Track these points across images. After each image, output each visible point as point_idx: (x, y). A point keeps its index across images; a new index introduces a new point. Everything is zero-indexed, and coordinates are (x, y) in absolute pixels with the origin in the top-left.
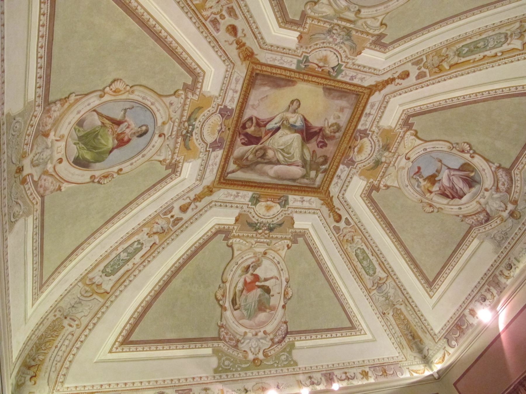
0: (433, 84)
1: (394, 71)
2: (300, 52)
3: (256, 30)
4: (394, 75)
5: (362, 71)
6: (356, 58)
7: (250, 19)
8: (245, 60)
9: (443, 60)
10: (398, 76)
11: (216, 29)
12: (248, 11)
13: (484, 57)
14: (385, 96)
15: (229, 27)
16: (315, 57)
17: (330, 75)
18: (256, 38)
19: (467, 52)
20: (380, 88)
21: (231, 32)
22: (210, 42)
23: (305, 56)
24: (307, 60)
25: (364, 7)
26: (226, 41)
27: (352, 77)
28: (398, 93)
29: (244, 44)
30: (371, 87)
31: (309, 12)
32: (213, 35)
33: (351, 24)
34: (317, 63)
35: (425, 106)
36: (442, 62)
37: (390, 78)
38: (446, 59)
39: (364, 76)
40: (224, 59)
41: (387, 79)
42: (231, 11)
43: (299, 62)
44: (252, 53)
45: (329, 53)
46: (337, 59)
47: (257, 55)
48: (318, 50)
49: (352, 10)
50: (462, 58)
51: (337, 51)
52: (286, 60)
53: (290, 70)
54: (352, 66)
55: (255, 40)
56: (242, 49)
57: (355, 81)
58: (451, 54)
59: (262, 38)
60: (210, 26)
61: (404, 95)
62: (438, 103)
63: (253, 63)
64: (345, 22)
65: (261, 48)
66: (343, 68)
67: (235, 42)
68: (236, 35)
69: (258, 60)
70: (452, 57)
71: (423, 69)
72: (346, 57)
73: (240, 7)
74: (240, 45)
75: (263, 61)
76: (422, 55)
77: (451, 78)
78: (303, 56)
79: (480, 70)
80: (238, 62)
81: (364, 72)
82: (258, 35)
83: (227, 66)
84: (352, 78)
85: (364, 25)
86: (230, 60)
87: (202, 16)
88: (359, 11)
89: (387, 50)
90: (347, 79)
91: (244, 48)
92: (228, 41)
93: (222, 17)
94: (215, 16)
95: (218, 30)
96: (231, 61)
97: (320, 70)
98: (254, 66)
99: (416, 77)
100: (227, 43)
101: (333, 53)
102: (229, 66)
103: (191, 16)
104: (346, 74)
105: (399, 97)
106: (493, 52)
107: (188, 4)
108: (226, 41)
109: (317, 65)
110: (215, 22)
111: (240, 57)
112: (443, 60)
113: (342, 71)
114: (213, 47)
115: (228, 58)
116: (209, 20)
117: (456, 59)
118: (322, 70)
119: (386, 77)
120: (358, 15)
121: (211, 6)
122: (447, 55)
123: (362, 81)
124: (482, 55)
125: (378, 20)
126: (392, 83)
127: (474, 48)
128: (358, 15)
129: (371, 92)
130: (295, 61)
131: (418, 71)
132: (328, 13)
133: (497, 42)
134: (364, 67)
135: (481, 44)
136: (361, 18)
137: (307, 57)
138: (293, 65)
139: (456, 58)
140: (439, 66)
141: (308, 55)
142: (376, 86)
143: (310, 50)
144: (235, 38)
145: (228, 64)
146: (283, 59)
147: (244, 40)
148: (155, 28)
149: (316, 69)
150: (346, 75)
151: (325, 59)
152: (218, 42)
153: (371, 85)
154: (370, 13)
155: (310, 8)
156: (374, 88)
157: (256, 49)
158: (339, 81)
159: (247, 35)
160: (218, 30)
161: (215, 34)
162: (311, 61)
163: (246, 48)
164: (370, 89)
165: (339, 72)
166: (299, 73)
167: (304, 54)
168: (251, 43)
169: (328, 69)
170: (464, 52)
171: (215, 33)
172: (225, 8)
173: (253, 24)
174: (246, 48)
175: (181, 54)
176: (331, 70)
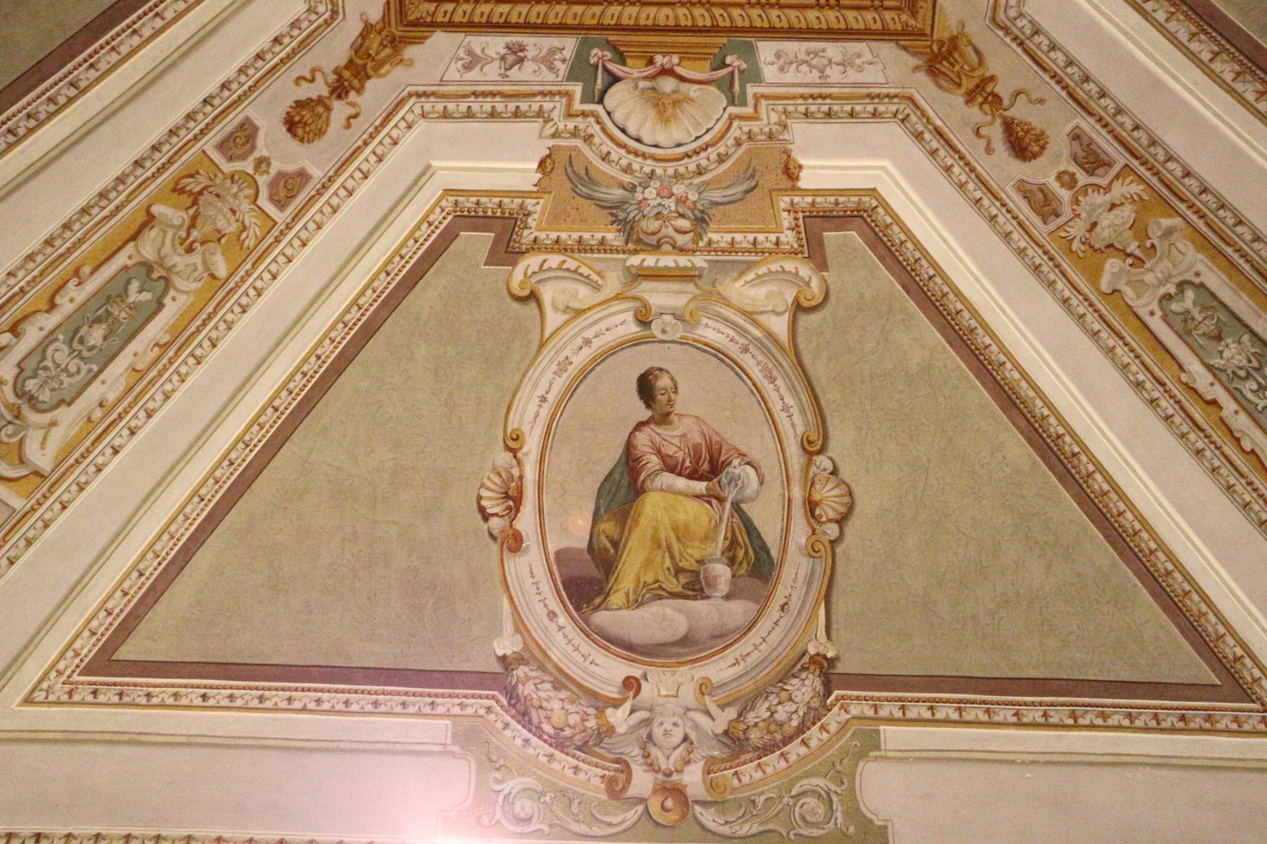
0: (172, 132)
1: (361, 127)
2: (769, 117)
3: (949, 161)
4: (353, 111)
5: (493, 94)
6: (551, 143)
7: (978, 194)
8: (954, 39)
9: (192, 225)
10: (328, 109)
11: (1085, 141)
12: (993, 218)
13: (52, 306)
14: (334, 13)
15: (1036, 149)
16: (705, 110)
17: (614, 47)
18: (939, 133)
19: (126, 290)
20: (374, 43)
21: (1027, 132)
22: (1103, 94)
23: (743, 103)
24: (726, 86)
25: (636, 342)
26: (1042, 101)
27: (521, 60)
28: (290, 45)
29: (970, 97)
30: (415, 32)
31: (805, 271)
32: (1092, 120)
33: (640, 267)
34: (685, 87)
35: (147, 32)
36: (194, 218)
37: (359, 91)
38: (183, 234)
39: (474, 75)
40: (1037, 39)
41: (370, 84)
42: (1045, 205)
43: (754, 75)
44: (932, 71)
45: (661, 138)
46: (617, 116)
47: (916, 69)
48: (707, 138)
49: (668, 318)
50: (130, 263)
51: (636, 154)
52: (804, 68)
53: (772, 32)
54: (547, 106)
55: (938, 123)
56: (976, 81)
57: (496, 44)
58: (179, 260)
59: (918, 136)
60: (1109, 149)
61: (263, 42)
62: (103, 66)
63: (920, 34)
64: (667, 268)
65: (911, 99)
66: (577, 89)
67: (1006, 102)
68: (1008, 126)
69: (905, 48)
70: (167, 249)
71: (248, 166)
72: (588, 138)
73: (1020, 224)
74: (982, 92)
75: (887, 49)
76: (296, 217)
77: (121, 180)
78: (750, 101)
79: (31, 257)
80: (978, 30)
81: (485, 94)
82: (935, 145)
83: (1021, 15)
84: (516, 56)
85: (594, 277)
86: (1015, 39)
87: (1141, 179)
88: (644, 323)
89: (447, 204)
90: (534, 44)
91: (969, 84)
92: (1030, 101)
93: (1067, 180)
94: (1093, 180)
95: (1076, 136)
96: (1007, 31)
97: (659, 59)
98: (912, 22)
99: (256, 129)
100: (1034, 97)
101: (646, 139)
102: (1012, 13)
103: (1170, 165)
104: (551, 68)
105: (279, 26)
106: (32, 335)
107: (1202, 217)
108: (1042, 101)
109: (682, 79)
110: (1093, 161)
111: (977, 52)
112: (192, 225)
113: (572, 76)
114: (1087, 79)
115: (1021, 44)
116: (1117, 168)
117: (147, 248)
118: (651, 62)
119: (376, 93)
120: (638, 304)
121: (1115, 212)
122: (190, 250)
123: (470, 52)
124: (66, 306)
125: (556, 308)
126: (337, 72)
127: (108, 313)
128: (638, 304)
129: (402, 12)
130: (770, 73)
131: (262, 151)
132: (741, 282)
133: (46, 368)
134: (493, 115)
135: (96, 336)
136: (618, 297)
137: (732, 102)
138: (771, 58)
139: (148, 253)
140: (195, 203)
141: (732, 110)
142: (397, 44)
143: (735, 132)
144: (1007, 114)
145: (1020, 23)
146: (816, 73)
147: (975, 114)
148: (1216, 49)
149: (675, 59)
150: (547, 61)
151: (663, 108)
152: (1071, 95)
153: (421, 40)
154: (602, 325)
155: (808, 284)
156: (397, 30)
157: (922, 87)
158: (562, 28)
159: (972, 136)
160: (1076, 136)
161: (1087, 125)
162: (712, 89)
163: (959, 85)
164: (415, 24)
165: (580, 69)
166: (734, 30)
167: (749, 110)
168: (949, 108)
169: (634, 69)
170: (135, 285)
171: (1084, 125)
172: (1067, 212)
173: (963, 178)
174: (959, 85)
175: (1216, 54)
176: (615, 68)
